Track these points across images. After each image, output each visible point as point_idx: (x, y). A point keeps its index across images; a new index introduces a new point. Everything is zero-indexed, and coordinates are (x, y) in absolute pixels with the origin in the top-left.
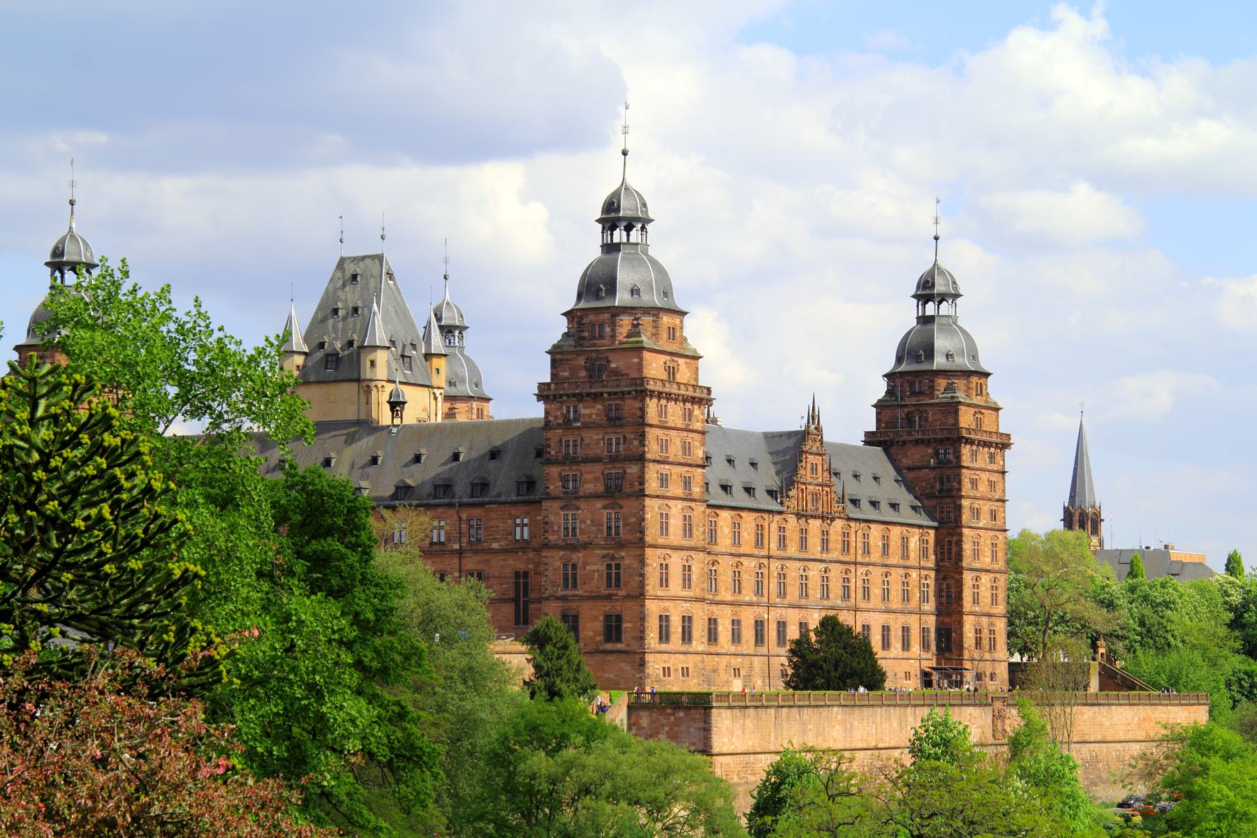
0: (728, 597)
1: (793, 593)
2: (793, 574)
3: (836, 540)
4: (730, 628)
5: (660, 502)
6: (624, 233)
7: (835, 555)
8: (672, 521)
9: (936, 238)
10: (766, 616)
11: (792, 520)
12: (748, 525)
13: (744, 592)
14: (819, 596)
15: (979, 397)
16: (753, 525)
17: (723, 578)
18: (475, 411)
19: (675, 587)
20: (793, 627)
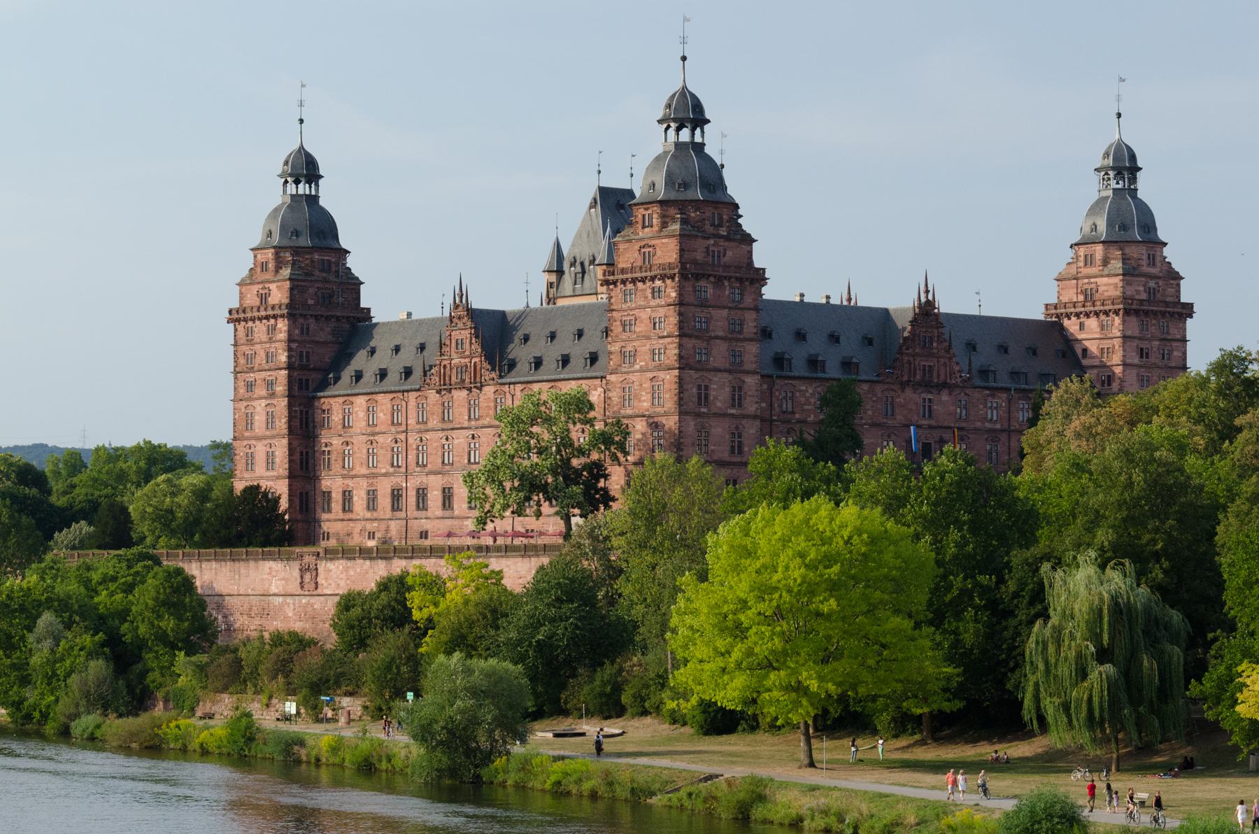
0: (364, 471)
1: (434, 462)
2: (435, 444)
3: (488, 407)
4: (365, 497)
5: (245, 404)
6: (294, 186)
7: (486, 421)
8: (257, 418)
9: (684, 59)
10: (404, 485)
11: (432, 395)
12: (384, 407)
13: (380, 465)
14: (466, 461)
15: (647, 230)
16: (389, 406)
17: (357, 455)
18: (1082, 259)
19: (260, 469)
20: (435, 493)
